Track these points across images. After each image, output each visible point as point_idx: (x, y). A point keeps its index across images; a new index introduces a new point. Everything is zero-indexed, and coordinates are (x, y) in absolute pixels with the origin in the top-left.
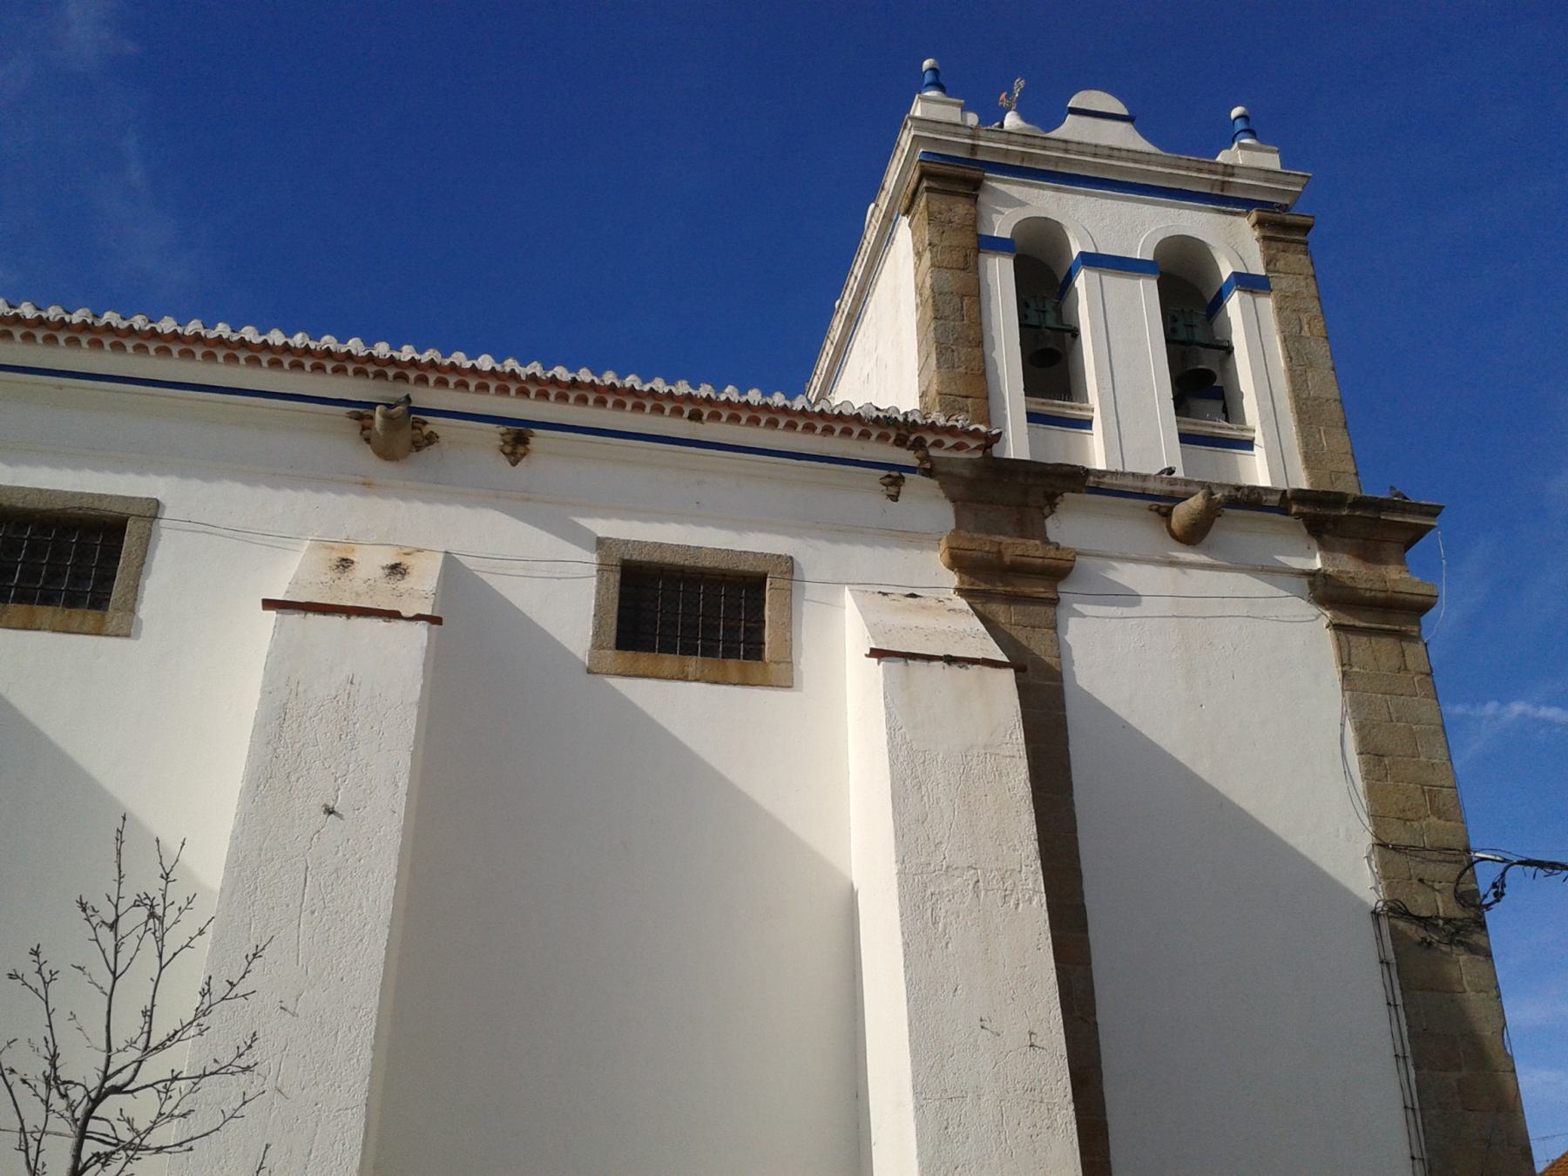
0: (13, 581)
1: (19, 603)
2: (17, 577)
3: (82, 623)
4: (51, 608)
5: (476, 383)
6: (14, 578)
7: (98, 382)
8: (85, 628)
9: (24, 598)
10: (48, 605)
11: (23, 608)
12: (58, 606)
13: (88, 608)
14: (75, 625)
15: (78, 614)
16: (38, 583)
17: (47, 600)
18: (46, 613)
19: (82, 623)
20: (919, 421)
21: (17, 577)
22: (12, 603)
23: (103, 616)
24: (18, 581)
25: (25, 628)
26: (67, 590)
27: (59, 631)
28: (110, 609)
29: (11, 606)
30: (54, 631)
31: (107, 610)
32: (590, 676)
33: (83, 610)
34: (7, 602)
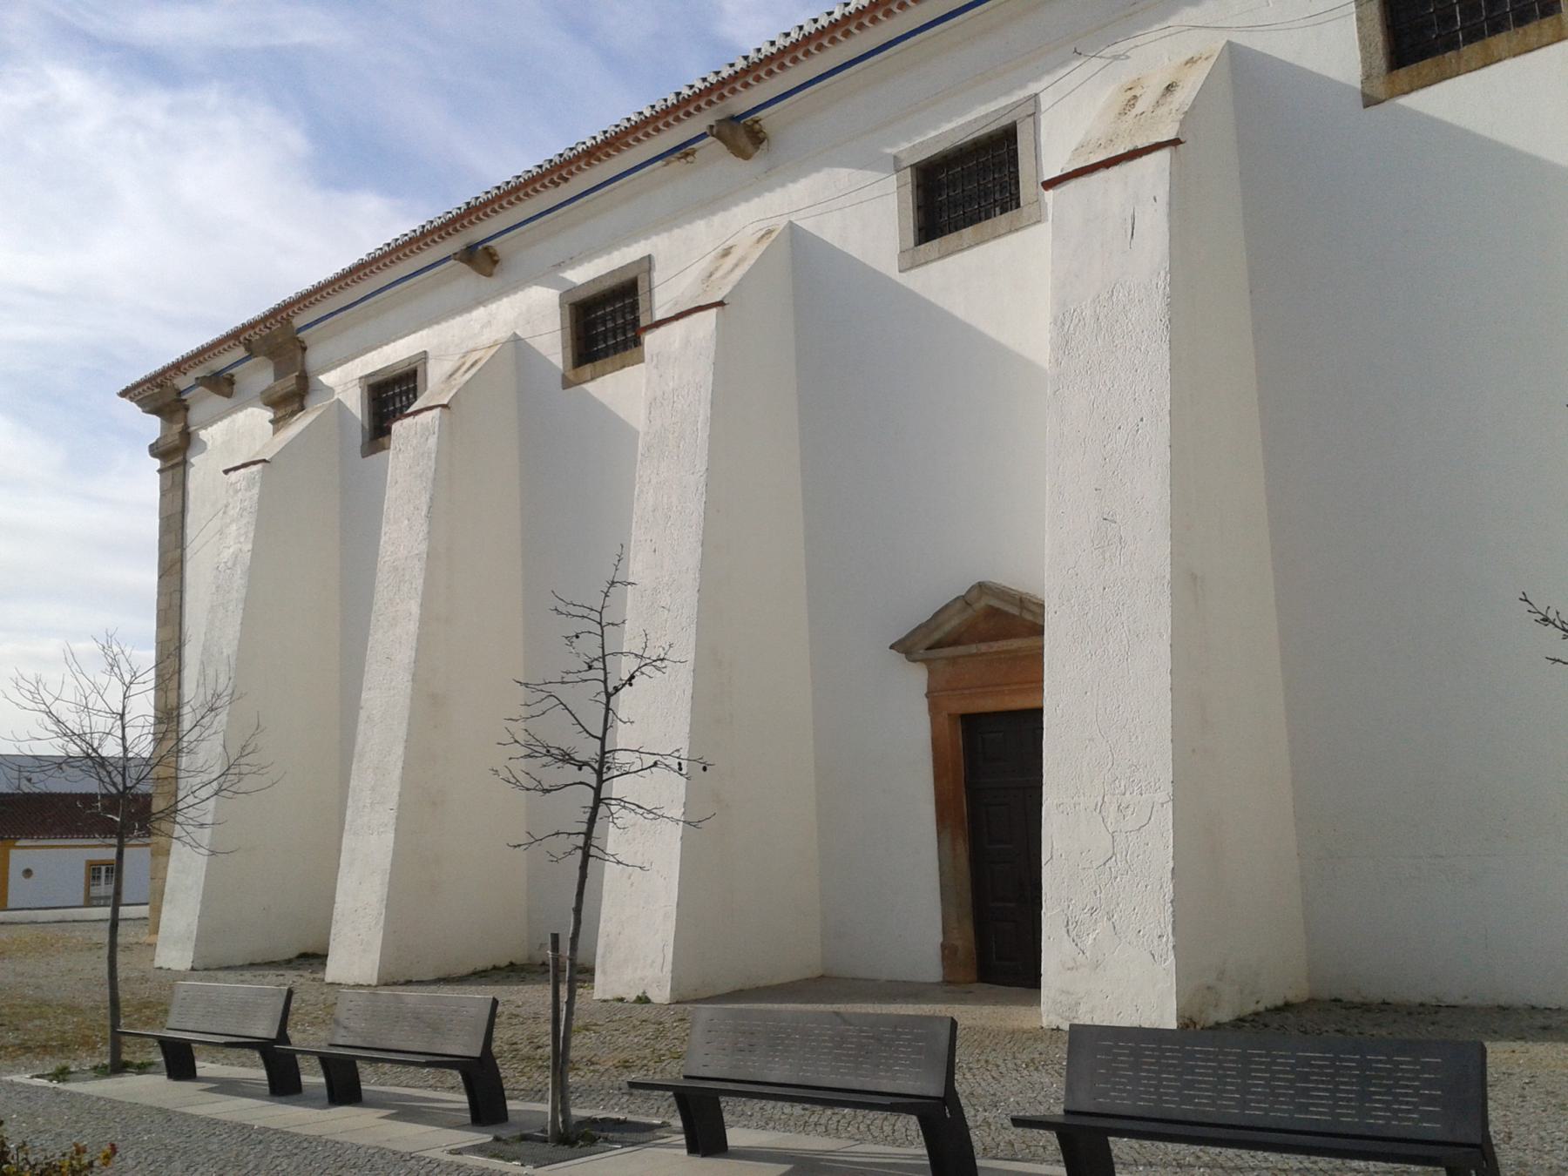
0: (1457, 25)
1: (1471, 42)
2: (1459, 19)
3: (1540, 35)
4: (1503, 35)
5: (764, 72)
6: (1457, 22)
7: (966, 14)
8: (1545, 40)
9: (1473, 36)
10: (1499, 32)
11: (1476, 46)
12: (1510, 29)
13: (1541, 18)
14: (1533, 39)
15: (1531, 28)
16: (1482, 15)
17: (1497, 28)
18: (1499, 41)
19: (1540, 35)
20: (628, 125)
21: (1459, 19)
22: (1464, 45)
23: (1560, 20)
24: (1461, 23)
25: (1485, 65)
26: (1512, 10)
27: (1520, 54)
28: (1563, 10)
29: (1464, 49)
30: (1515, 56)
31: (1561, 12)
32: (1373, 109)
33: (1536, 23)
34: (1460, 48)
